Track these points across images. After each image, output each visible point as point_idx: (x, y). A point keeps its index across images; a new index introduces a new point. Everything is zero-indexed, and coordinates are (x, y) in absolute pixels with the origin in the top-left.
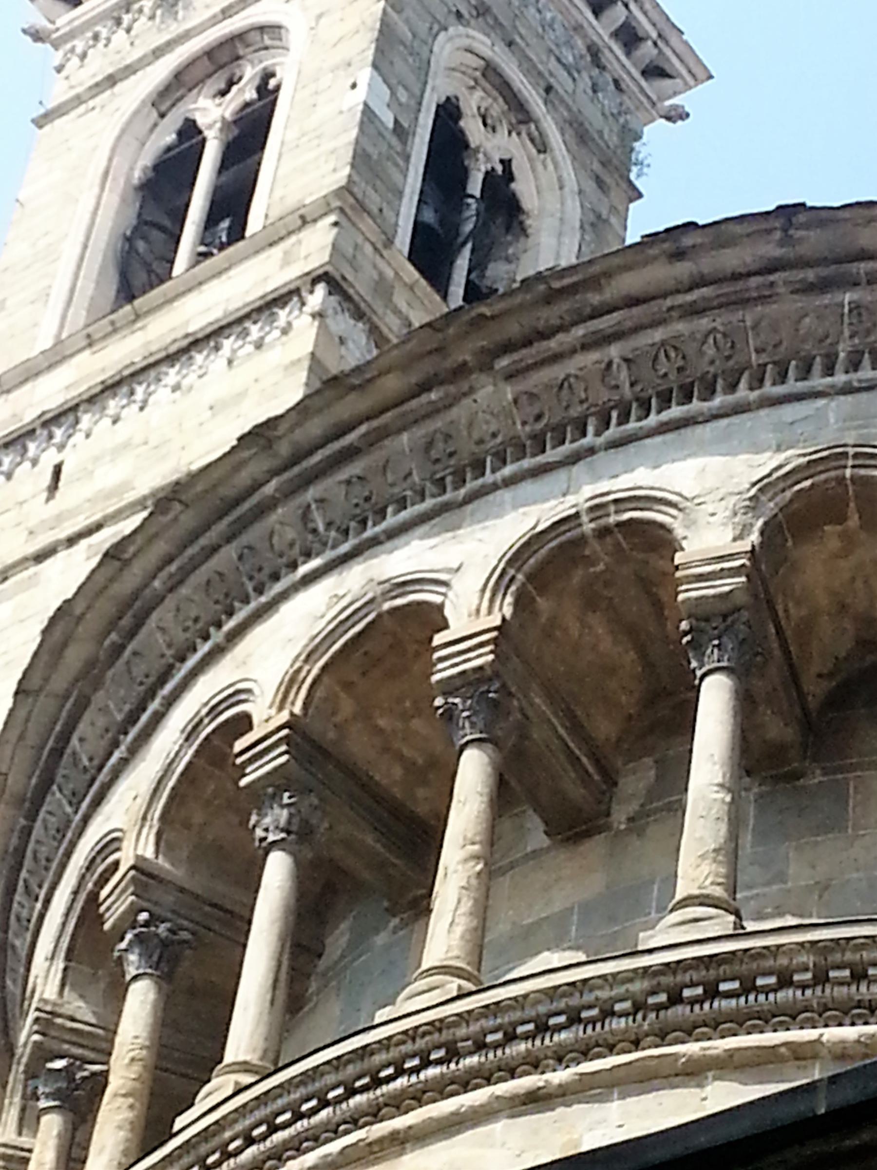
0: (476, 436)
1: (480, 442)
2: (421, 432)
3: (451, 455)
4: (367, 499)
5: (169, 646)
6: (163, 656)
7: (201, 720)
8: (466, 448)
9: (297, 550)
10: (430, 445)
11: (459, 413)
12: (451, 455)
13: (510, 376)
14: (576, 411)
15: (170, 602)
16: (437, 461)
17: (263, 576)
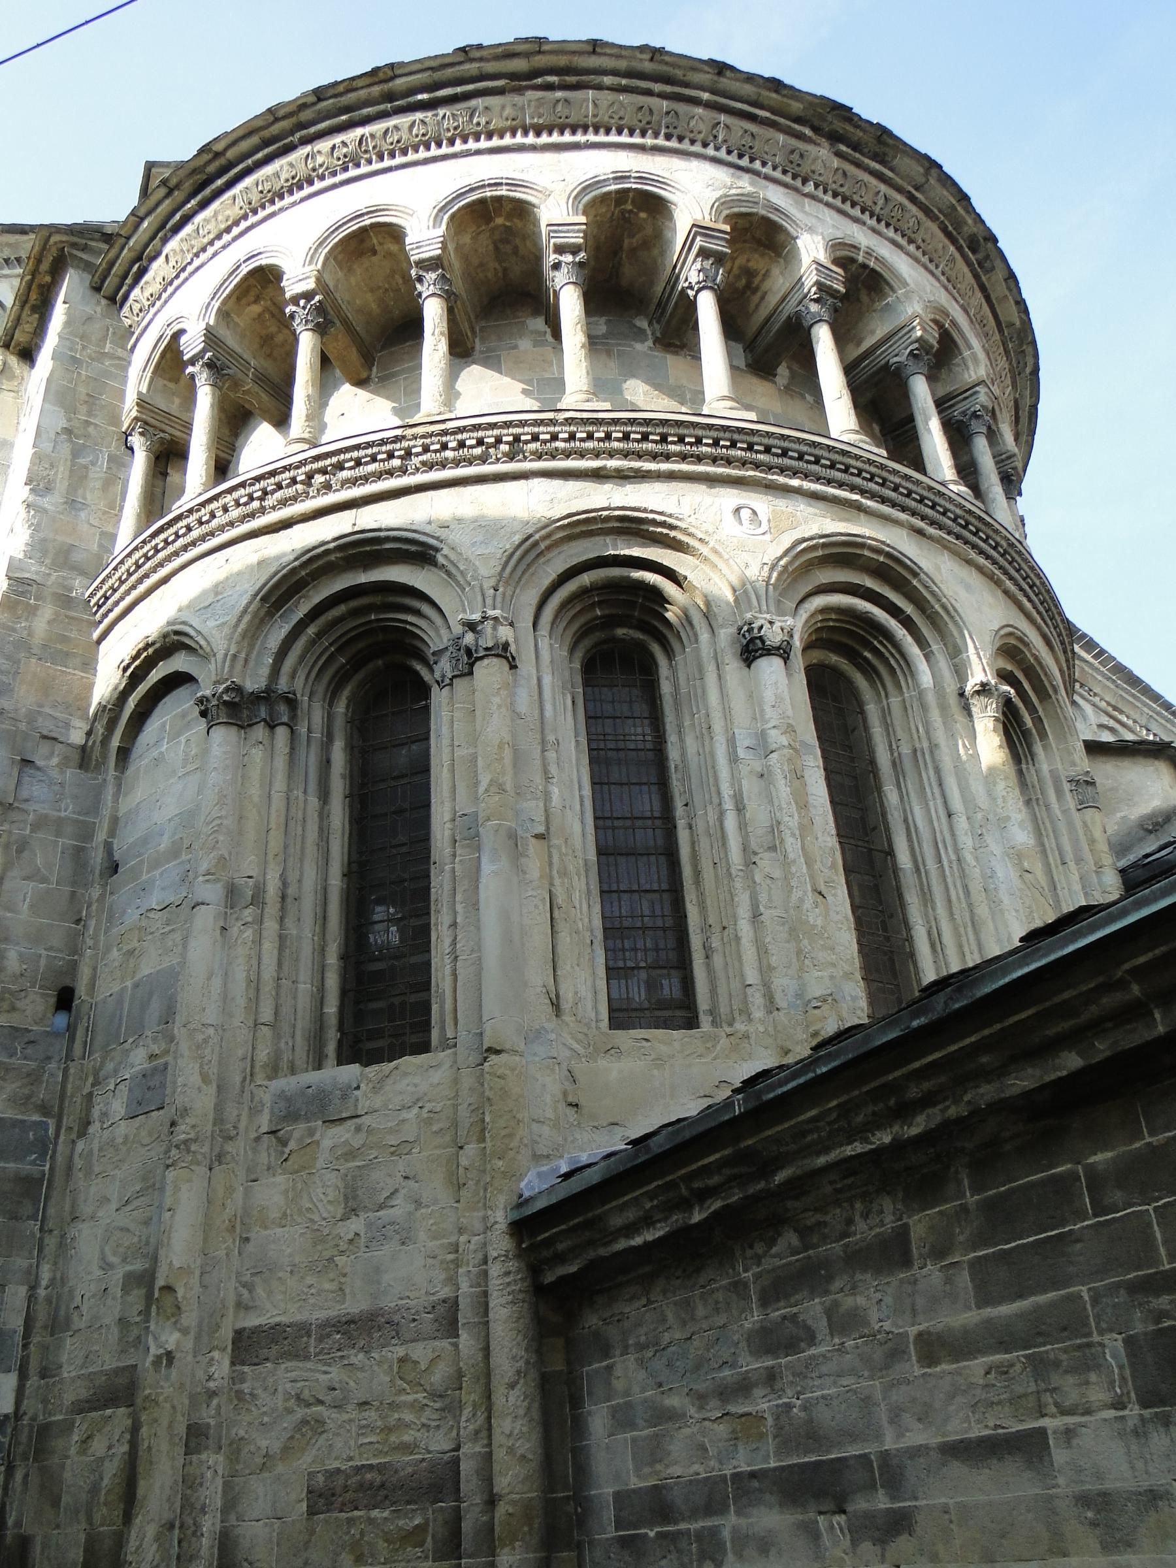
0: (813, 168)
1: (813, 172)
2: (794, 142)
3: (799, 165)
4: (751, 148)
5: (595, 116)
6: (586, 116)
7: (629, 177)
8: (805, 169)
9: (702, 136)
10: (792, 152)
11: (810, 147)
12: (799, 165)
13: (839, 154)
14: (856, 198)
15: (606, 97)
16: (791, 162)
17: (676, 132)
